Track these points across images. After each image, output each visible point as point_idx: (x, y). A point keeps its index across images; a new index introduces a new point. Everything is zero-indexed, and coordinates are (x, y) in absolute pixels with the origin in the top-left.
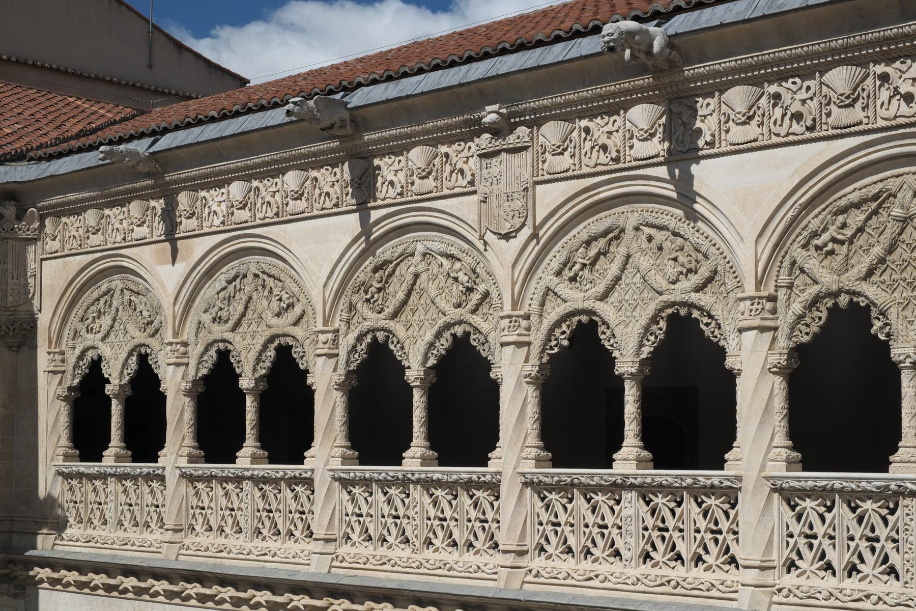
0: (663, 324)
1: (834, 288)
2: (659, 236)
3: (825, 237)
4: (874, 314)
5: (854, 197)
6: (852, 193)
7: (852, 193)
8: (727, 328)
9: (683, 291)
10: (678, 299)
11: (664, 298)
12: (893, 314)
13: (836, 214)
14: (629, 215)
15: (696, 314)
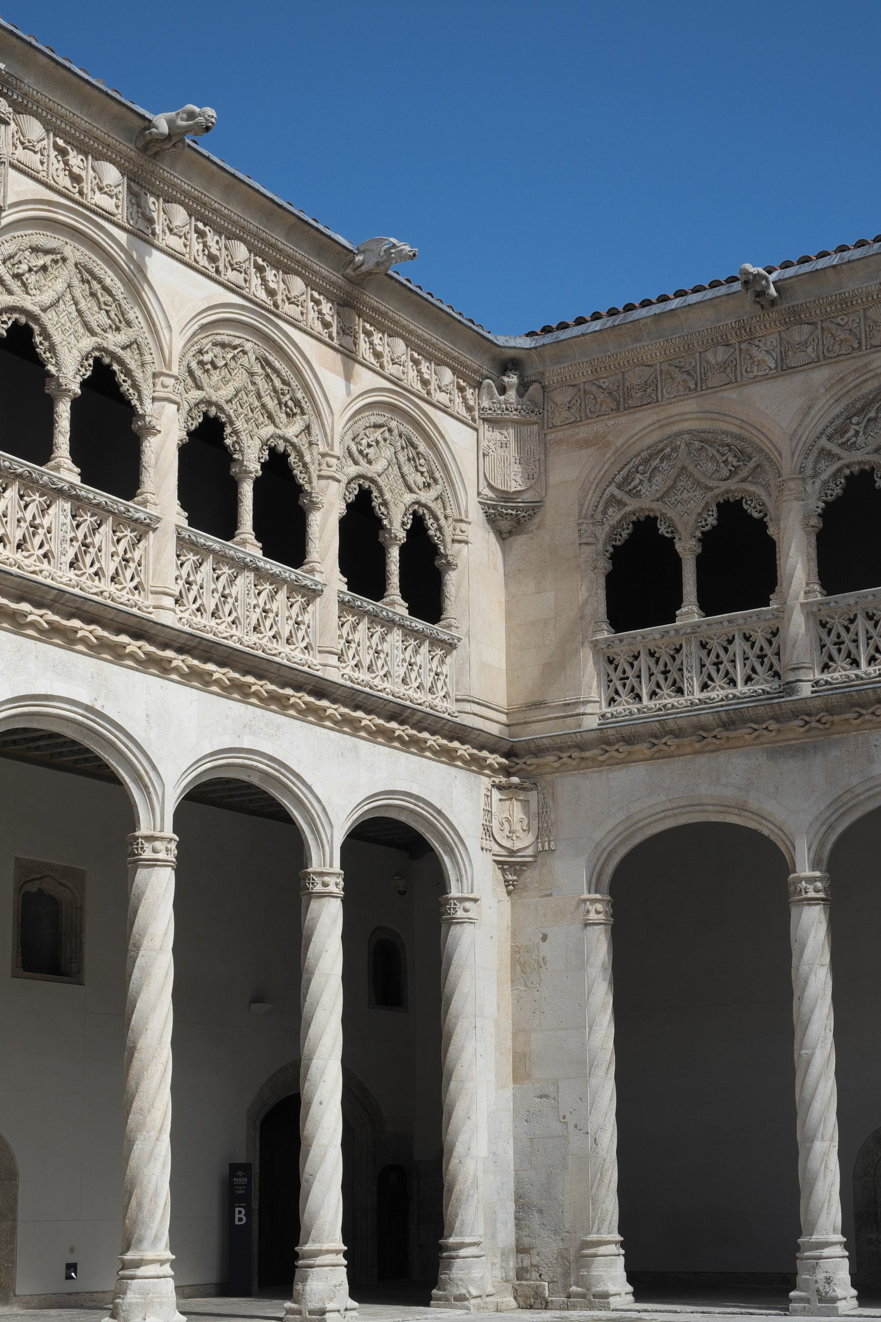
0: (91, 361)
1: (214, 399)
2: (96, 286)
3: (207, 358)
4: (228, 430)
5: (226, 339)
6: (225, 335)
7: (225, 335)
8: (147, 392)
9: (113, 341)
10: (112, 348)
11: (99, 340)
12: (244, 437)
13: (215, 344)
14: (73, 251)
15: (116, 367)
